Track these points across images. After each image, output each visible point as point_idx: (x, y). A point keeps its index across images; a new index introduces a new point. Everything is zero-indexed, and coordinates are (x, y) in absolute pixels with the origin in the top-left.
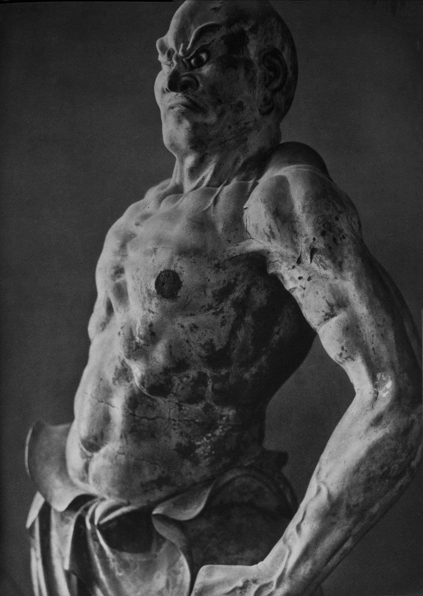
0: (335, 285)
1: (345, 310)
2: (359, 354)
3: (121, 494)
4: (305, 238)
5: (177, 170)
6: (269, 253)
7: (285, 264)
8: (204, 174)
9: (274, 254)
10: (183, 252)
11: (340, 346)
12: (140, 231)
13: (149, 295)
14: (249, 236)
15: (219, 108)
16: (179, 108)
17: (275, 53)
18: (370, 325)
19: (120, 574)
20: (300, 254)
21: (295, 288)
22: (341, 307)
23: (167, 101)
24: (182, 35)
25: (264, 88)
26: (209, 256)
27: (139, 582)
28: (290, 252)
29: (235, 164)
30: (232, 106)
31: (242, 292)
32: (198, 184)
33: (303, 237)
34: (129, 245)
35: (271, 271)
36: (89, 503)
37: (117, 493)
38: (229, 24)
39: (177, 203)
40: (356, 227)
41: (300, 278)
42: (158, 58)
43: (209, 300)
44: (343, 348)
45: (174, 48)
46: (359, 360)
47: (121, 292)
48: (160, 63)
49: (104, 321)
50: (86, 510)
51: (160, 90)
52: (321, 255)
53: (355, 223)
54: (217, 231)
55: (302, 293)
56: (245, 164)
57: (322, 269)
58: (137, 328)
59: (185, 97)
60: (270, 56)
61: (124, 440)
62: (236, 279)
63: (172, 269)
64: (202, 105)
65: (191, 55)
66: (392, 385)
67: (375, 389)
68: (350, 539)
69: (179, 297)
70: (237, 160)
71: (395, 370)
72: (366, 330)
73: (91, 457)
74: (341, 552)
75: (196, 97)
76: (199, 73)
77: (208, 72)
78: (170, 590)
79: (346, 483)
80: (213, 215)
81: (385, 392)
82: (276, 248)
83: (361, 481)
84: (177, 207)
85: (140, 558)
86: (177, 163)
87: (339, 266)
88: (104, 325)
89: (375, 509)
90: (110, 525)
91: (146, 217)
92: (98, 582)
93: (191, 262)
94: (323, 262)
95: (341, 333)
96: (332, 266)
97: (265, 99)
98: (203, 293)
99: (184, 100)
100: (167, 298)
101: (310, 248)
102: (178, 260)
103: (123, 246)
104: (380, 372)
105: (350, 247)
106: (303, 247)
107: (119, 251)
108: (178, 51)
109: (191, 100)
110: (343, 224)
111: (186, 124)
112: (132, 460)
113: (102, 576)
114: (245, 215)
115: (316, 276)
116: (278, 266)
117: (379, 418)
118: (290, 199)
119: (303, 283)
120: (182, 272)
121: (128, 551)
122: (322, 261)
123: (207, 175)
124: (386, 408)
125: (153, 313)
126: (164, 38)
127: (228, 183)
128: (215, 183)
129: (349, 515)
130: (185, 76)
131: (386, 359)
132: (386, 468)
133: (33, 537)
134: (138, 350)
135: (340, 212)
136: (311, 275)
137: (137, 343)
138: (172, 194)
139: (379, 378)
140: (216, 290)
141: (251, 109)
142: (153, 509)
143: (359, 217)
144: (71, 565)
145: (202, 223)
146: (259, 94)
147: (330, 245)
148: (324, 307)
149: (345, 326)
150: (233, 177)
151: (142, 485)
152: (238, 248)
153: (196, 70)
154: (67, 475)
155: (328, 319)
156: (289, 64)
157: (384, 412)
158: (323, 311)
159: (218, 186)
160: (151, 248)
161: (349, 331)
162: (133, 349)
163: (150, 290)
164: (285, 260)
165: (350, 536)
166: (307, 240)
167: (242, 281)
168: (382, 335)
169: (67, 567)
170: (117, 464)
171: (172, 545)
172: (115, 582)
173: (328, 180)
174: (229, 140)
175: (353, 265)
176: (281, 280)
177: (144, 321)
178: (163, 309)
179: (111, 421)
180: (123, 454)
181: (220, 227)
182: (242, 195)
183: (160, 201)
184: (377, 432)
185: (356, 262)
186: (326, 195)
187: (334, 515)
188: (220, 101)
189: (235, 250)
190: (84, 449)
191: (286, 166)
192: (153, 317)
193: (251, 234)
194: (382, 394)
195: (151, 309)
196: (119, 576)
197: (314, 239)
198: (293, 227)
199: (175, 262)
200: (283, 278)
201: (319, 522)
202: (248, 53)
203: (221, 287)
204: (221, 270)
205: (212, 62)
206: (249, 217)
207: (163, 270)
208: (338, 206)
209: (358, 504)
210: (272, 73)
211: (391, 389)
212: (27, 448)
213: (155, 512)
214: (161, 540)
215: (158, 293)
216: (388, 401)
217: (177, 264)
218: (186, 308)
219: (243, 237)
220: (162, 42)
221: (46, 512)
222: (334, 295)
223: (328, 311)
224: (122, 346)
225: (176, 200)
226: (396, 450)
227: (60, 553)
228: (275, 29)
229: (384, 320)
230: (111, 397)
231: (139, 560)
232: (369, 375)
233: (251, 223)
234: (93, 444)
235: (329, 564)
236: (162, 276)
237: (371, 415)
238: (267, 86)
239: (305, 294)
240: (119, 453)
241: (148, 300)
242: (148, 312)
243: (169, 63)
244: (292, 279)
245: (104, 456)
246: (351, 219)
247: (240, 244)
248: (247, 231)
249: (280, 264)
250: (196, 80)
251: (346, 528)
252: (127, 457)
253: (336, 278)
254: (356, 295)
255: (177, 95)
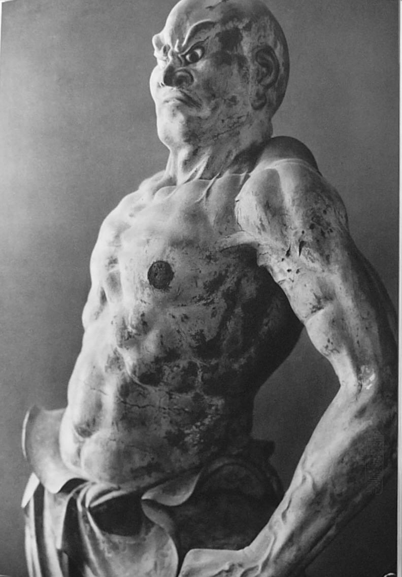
0: (322, 278)
1: (331, 302)
2: (344, 347)
3: (112, 479)
4: (294, 231)
5: (170, 163)
6: (259, 245)
7: (275, 256)
8: (197, 166)
9: (265, 246)
10: (175, 243)
11: (327, 338)
12: (133, 222)
13: (142, 285)
14: (239, 227)
15: (213, 102)
16: (174, 102)
17: (269, 50)
18: (355, 318)
19: (110, 555)
20: (289, 247)
21: (284, 280)
22: (328, 299)
23: (163, 96)
24: (178, 30)
25: (257, 83)
26: (201, 248)
27: (128, 563)
28: (279, 245)
29: (227, 157)
30: (225, 100)
31: (232, 284)
32: (191, 176)
33: (293, 230)
34: (122, 236)
35: (261, 263)
36: (81, 486)
37: (108, 477)
38: (224, 22)
39: (170, 195)
40: (343, 221)
41: (289, 271)
42: (153, 53)
43: (199, 291)
44: (329, 341)
45: (170, 45)
46: (344, 352)
47: (114, 281)
48: (156, 58)
49: (97, 310)
50: (78, 492)
51: (156, 85)
52: (310, 248)
53: (342, 217)
54: (209, 223)
55: (291, 286)
56: (237, 158)
57: (310, 262)
58: (129, 319)
59: (181, 91)
60: (263, 53)
61: (116, 428)
62: (227, 271)
63: (165, 260)
64: (196, 99)
65: (187, 51)
66: (376, 377)
67: (359, 381)
68: (334, 527)
69: (171, 287)
70: (230, 152)
71: (378, 363)
72: (351, 322)
73: (83, 442)
74: (324, 539)
75: (190, 91)
76: (194, 68)
77: (202, 67)
78: (158, 572)
79: (330, 473)
80: (205, 207)
81: (368, 384)
82: (267, 242)
83: (345, 471)
84: (170, 198)
85: (130, 541)
86: (171, 156)
87: (327, 259)
88: (97, 314)
89: (358, 499)
90: (101, 508)
91: (139, 208)
92: (87, 561)
93: (183, 253)
94: (312, 255)
95: (327, 325)
96: (320, 259)
97: (257, 94)
98: (194, 284)
99: (179, 95)
100: (159, 289)
101: (299, 240)
102: (170, 251)
103: (117, 237)
104: (364, 364)
105: (338, 240)
106: (292, 240)
107: (113, 242)
108: (174, 47)
109: (185, 95)
110: (330, 218)
111: (181, 117)
112: (123, 446)
113: (92, 556)
114: (236, 208)
115: (304, 269)
116: (268, 258)
117: (362, 411)
118: (280, 193)
119: (292, 275)
120: (173, 263)
121: (118, 534)
122: (311, 254)
123: (200, 167)
124: (370, 400)
125: (145, 303)
126: (160, 34)
127: (220, 176)
128: (208, 175)
129: (332, 505)
130: (179, 71)
131: (370, 352)
132: (368, 460)
133: (28, 516)
134: (130, 339)
135: (328, 206)
136: (299, 268)
137: (129, 333)
138: (165, 186)
139: (363, 372)
140: (207, 282)
141: (245, 104)
142: (142, 494)
143: (346, 211)
144: (63, 545)
145: (194, 215)
146: (252, 89)
147: (318, 239)
148: (312, 299)
149: (332, 319)
150: (226, 170)
151: (132, 471)
152: (229, 240)
153: (191, 66)
154: (60, 457)
155: (315, 311)
156: (281, 61)
157: (368, 404)
158: (311, 304)
159: (211, 179)
160: (144, 239)
161: (335, 324)
162: (125, 338)
163: (143, 281)
164: (275, 253)
165: (334, 524)
166: (296, 233)
167: (233, 273)
168: (367, 328)
169: (59, 545)
170: (108, 450)
171: (161, 529)
172: (104, 562)
173: (317, 174)
174: (223, 134)
175: (339, 259)
176: (271, 272)
177: (136, 311)
178: (155, 299)
179: (103, 408)
180: (115, 440)
181: (212, 219)
182: (234, 187)
183: (154, 194)
184: (360, 424)
185: (343, 256)
186: (315, 188)
187: (318, 503)
188: (214, 96)
189: (226, 241)
190: (77, 435)
191: (277, 160)
192: (145, 307)
193: (242, 226)
194: (365, 387)
195: (143, 299)
196: (109, 557)
197: (303, 232)
198: (282, 220)
199: (168, 251)
200: (272, 270)
201: (304, 510)
202: (242, 48)
203: (212, 279)
204: (212, 261)
205: (207, 58)
206: (240, 209)
207: (155, 261)
208: (327, 200)
209: (341, 493)
210: (264, 70)
211: (375, 382)
212: (24, 431)
213: (144, 497)
214: (150, 524)
215: (151, 283)
216: (371, 394)
217: (169, 255)
218: (177, 299)
219: (234, 230)
220: (158, 38)
221: (40, 493)
222: (321, 288)
223: (315, 304)
224: (114, 335)
225: (170, 191)
226: (378, 442)
227: (53, 532)
228: (268, 27)
229: (368, 314)
230: (104, 384)
231: (127, 542)
232: (354, 367)
233: (242, 215)
234: (86, 430)
235: (313, 550)
236: (155, 266)
237: (355, 407)
238: (260, 82)
239: (294, 286)
240: (111, 440)
241: (141, 290)
242: (140, 302)
243: (165, 58)
244: (282, 271)
245: (96, 442)
246: (339, 213)
247: (231, 236)
248: (238, 224)
249: (269, 256)
250: (191, 76)
251: (330, 516)
252: (118, 443)
253: (323, 271)
254: (342, 287)
255: (172, 89)
